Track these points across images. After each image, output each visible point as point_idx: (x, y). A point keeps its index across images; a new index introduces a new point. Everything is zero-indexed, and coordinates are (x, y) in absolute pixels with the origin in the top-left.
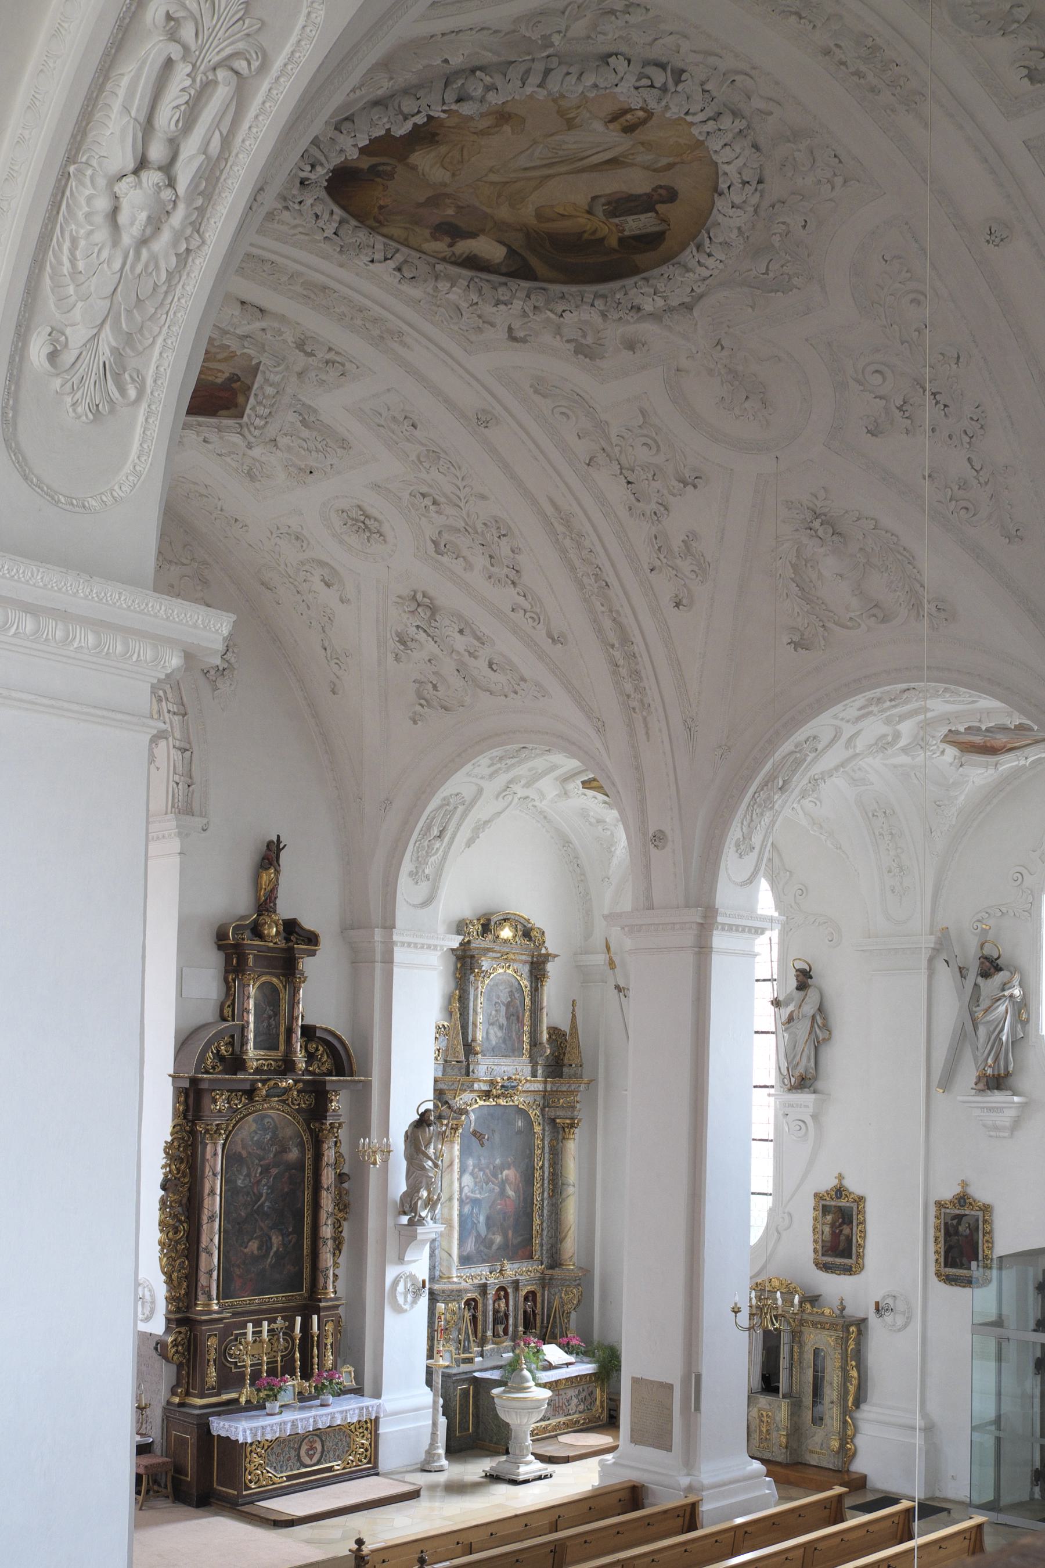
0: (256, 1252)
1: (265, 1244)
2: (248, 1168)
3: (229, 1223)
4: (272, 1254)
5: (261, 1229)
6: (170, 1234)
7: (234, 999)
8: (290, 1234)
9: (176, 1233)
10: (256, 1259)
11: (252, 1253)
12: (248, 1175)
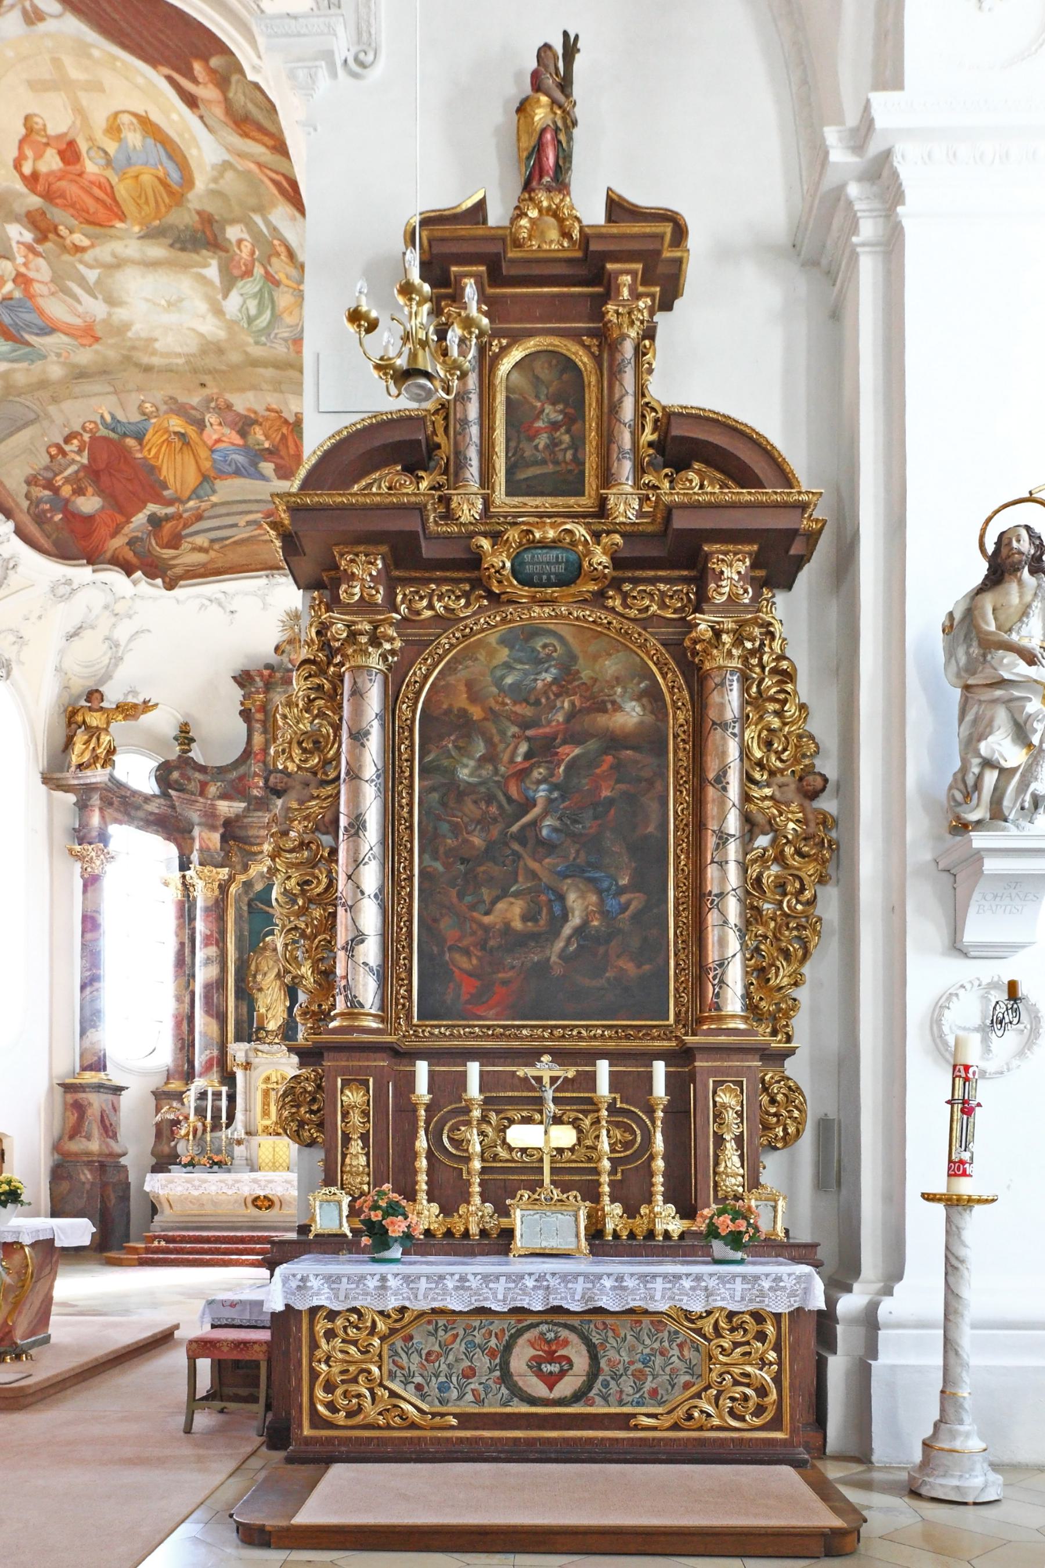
1: (549, 910)
4: (567, 930)
5: (533, 875)
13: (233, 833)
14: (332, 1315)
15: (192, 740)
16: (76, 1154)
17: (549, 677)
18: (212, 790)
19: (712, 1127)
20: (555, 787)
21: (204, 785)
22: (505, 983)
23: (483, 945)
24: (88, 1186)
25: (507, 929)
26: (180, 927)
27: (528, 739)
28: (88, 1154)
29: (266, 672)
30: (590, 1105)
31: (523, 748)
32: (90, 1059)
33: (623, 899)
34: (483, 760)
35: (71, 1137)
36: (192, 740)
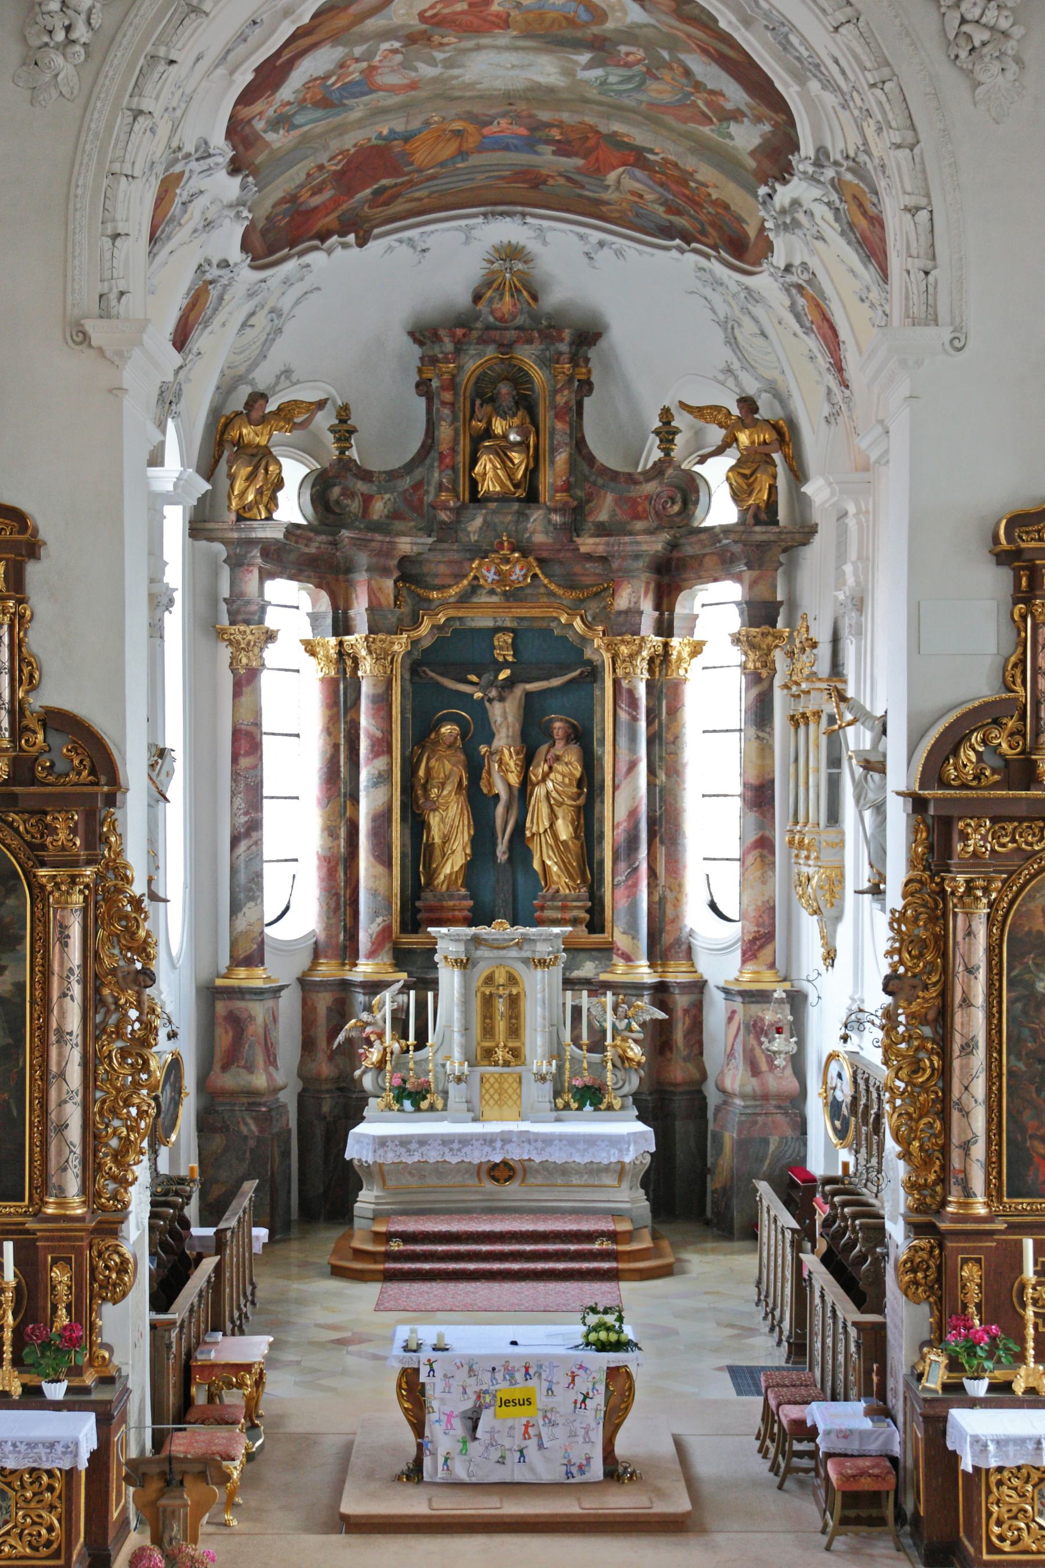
3: (1019, 1058)
6: (903, 1074)
7: (1025, 652)
9: (915, 1072)
13: (409, 574)
14: (1000, 1469)
16: (233, 1094)
18: (379, 508)
21: (367, 499)
24: (252, 1143)
28: (252, 1093)
32: (247, 948)
35: (225, 1068)
36: (352, 431)
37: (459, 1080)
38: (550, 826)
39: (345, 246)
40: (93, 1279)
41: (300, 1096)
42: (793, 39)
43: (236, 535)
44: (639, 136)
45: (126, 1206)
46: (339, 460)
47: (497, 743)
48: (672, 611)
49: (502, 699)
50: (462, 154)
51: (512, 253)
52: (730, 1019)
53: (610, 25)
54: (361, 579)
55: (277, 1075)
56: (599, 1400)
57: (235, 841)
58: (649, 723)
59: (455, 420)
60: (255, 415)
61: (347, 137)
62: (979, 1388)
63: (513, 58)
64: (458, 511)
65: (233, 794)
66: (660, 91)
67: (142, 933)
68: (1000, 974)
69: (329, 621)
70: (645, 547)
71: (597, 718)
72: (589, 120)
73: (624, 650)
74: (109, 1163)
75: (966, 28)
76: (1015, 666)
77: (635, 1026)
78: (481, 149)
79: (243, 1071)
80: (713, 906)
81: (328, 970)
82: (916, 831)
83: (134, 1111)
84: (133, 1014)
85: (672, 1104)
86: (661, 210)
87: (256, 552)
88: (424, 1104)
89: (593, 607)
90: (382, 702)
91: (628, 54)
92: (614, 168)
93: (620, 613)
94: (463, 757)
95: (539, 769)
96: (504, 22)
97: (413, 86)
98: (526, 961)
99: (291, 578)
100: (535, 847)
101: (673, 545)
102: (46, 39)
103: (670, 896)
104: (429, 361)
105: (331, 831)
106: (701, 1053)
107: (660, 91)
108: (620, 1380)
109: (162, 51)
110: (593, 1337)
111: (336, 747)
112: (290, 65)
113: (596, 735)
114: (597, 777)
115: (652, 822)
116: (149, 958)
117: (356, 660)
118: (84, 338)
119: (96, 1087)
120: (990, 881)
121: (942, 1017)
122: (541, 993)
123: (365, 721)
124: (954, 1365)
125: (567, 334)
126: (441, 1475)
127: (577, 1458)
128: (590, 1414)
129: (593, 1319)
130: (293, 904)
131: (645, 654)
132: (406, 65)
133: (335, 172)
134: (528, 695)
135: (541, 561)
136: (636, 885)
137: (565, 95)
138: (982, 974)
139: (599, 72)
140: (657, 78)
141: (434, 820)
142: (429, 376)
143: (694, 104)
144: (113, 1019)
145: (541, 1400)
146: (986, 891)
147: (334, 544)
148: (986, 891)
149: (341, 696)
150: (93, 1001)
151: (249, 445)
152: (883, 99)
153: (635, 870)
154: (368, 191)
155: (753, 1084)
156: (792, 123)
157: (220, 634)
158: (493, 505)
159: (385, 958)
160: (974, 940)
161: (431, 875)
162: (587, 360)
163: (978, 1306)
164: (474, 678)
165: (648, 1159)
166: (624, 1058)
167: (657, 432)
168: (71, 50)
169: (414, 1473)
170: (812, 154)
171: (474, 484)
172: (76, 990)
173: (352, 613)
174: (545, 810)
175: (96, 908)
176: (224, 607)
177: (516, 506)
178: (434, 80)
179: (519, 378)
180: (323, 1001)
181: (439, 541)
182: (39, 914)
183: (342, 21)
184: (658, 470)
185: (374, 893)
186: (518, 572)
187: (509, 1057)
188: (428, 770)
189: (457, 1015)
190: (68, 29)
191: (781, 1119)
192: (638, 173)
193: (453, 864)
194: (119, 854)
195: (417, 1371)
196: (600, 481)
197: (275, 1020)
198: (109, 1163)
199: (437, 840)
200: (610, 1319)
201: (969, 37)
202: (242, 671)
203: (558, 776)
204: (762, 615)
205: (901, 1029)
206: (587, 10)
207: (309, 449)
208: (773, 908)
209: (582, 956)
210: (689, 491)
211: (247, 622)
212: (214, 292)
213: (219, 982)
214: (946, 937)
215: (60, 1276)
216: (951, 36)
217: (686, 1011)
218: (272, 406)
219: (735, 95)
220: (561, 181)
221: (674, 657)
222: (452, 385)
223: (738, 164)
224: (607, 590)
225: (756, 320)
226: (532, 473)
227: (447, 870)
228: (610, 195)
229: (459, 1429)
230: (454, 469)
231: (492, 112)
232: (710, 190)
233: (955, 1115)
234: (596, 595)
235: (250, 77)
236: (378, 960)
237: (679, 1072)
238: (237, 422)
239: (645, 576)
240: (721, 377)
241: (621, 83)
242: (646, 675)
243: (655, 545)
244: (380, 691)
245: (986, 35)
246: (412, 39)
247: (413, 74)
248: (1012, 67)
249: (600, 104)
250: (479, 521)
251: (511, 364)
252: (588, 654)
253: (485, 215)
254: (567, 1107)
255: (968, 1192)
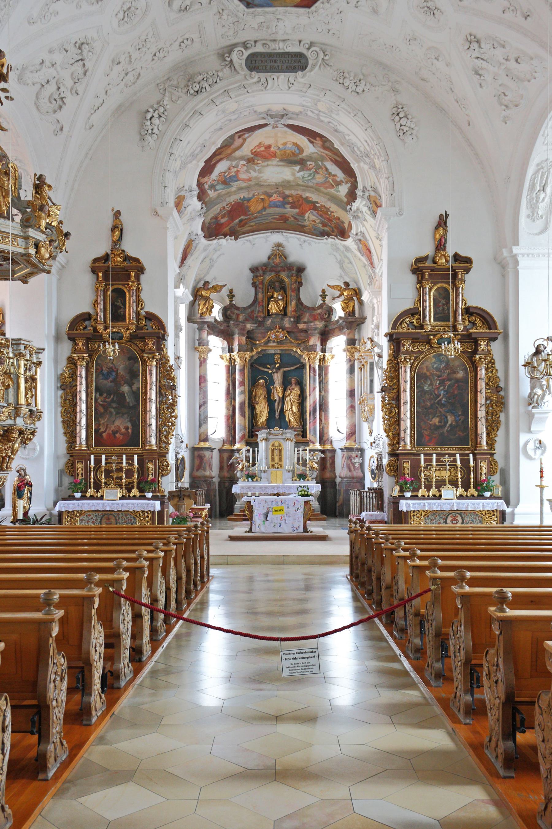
0: (437, 424)
2: (431, 381)
3: (420, 408)
4: (448, 425)
5: (440, 412)
6: (387, 413)
8: (459, 416)
9: (390, 413)
10: (437, 428)
11: (435, 424)
12: (431, 384)
13: (250, 336)
15: (234, 296)
16: (200, 477)
17: (443, 365)
18: (241, 318)
19: (480, 471)
20: (445, 391)
21: (238, 315)
22: (435, 437)
23: (430, 429)
25: (435, 425)
26: (228, 377)
27: (439, 380)
28: (206, 477)
29: (264, 268)
30: (456, 466)
31: (438, 382)
32: (203, 437)
33: (460, 417)
34: (429, 385)
35: (197, 470)
36: (234, 296)
37: (265, 472)
38: (291, 408)
39: (231, 239)
40: (159, 469)
41: (219, 483)
42: (356, 149)
43: (200, 320)
44: (313, 197)
45: (168, 450)
46: (230, 304)
47: (275, 385)
48: (325, 346)
49: (277, 372)
50: (264, 208)
51: (279, 245)
52: (343, 457)
53: (304, 154)
54: (236, 337)
55: (214, 472)
56: (302, 510)
57: (200, 407)
58: (319, 378)
59: (263, 293)
60: (206, 288)
61: (231, 197)
62: (408, 495)
63: (278, 169)
64: (265, 317)
65: (200, 394)
66: (320, 178)
67: (172, 375)
68: (414, 385)
69: (227, 349)
70: (317, 326)
71: (304, 378)
72: (300, 193)
73: (312, 356)
74: (163, 438)
75: (402, 127)
76: (418, 301)
77: (315, 458)
78: (270, 207)
79: (203, 471)
80: (338, 430)
81: (227, 447)
82: (390, 346)
83: (170, 424)
84: (170, 397)
85: (327, 483)
86: (320, 226)
87: (206, 326)
88: (255, 480)
89: (303, 345)
90: (242, 371)
91: (310, 165)
92: (307, 212)
93: (311, 346)
94: (265, 389)
95: (288, 393)
96: (274, 155)
97: (249, 180)
98: (284, 439)
99: (216, 336)
100: (286, 415)
101: (326, 326)
102: (146, 132)
103: (325, 426)
104: (255, 277)
105: (228, 409)
106: (335, 470)
107: (320, 178)
108: (308, 506)
109: (178, 137)
110: (300, 493)
111: (229, 385)
112: (214, 166)
113: (304, 383)
114: (304, 395)
115: (320, 405)
116: (174, 382)
117: (235, 360)
118: (156, 213)
119: (160, 418)
120: (410, 357)
121: (398, 398)
122: (288, 448)
123: (238, 377)
124: (401, 490)
125: (295, 268)
126: (257, 530)
127: (296, 526)
128: (299, 513)
129: (300, 489)
130: (217, 430)
131: (318, 357)
132: (247, 171)
133: (228, 211)
134: (285, 372)
135: (288, 332)
136: (315, 422)
137: (294, 184)
138: (409, 383)
139: (302, 173)
140: (318, 173)
141: (257, 407)
142: (255, 281)
143: (329, 182)
144: (164, 399)
145: (285, 510)
146: (410, 359)
147: (228, 326)
148: (410, 359)
149: (231, 370)
150: (159, 394)
151: (204, 296)
152: (379, 148)
153: (315, 418)
154: (237, 220)
155: (349, 474)
156: (356, 181)
157: (195, 349)
158: (274, 316)
159: (243, 443)
160: (406, 374)
161: (256, 423)
162: (301, 276)
163: (408, 474)
164: (269, 366)
165: (319, 493)
166: (312, 467)
167: (321, 296)
168: (153, 135)
169: (251, 531)
170: (362, 188)
171: (268, 311)
172: (154, 388)
173: (233, 347)
174: (289, 404)
175: (160, 368)
176: (197, 341)
177: (281, 316)
178: (256, 178)
179: (281, 281)
180: (226, 455)
181: (259, 326)
182: (144, 368)
183: (229, 151)
184: (321, 306)
185: (240, 425)
186: (281, 335)
187: (279, 466)
188: (256, 393)
189: (264, 454)
190: (152, 130)
191: (357, 484)
192: (314, 212)
193: (263, 418)
194: (166, 353)
195: (250, 502)
196: (305, 310)
197: (212, 458)
198: (163, 438)
199: (258, 412)
200: (305, 489)
201: (403, 130)
202: (202, 359)
203: (294, 393)
204: (351, 342)
205: (386, 401)
206: (298, 149)
207: (221, 301)
208: (355, 425)
209: (300, 444)
210: (330, 311)
211: (204, 345)
212: (194, 244)
213: (196, 446)
214: (399, 375)
215: (150, 465)
216: (398, 130)
217: (330, 458)
218: (210, 286)
219: (340, 175)
220: (292, 219)
221: (326, 359)
222: (262, 283)
223: (342, 201)
224: (306, 341)
225: (348, 259)
226: (285, 308)
227: (261, 420)
228: (306, 223)
229: (263, 518)
230: (263, 306)
231: (272, 191)
232: (334, 214)
233: (402, 422)
234: (304, 342)
235: (203, 164)
236: (241, 443)
237: (328, 475)
238: (201, 290)
239: (318, 335)
240: (339, 278)
241: (308, 177)
242: (318, 363)
243: (320, 325)
244: (242, 368)
245: (407, 129)
246: (250, 161)
247: (250, 175)
248: (415, 138)
249: (303, 186)
250: (270, 321)
251: (278, 277)
252: (302, 360)
253: (271, 232)
254: (296, 480)
255: (405, 443)
